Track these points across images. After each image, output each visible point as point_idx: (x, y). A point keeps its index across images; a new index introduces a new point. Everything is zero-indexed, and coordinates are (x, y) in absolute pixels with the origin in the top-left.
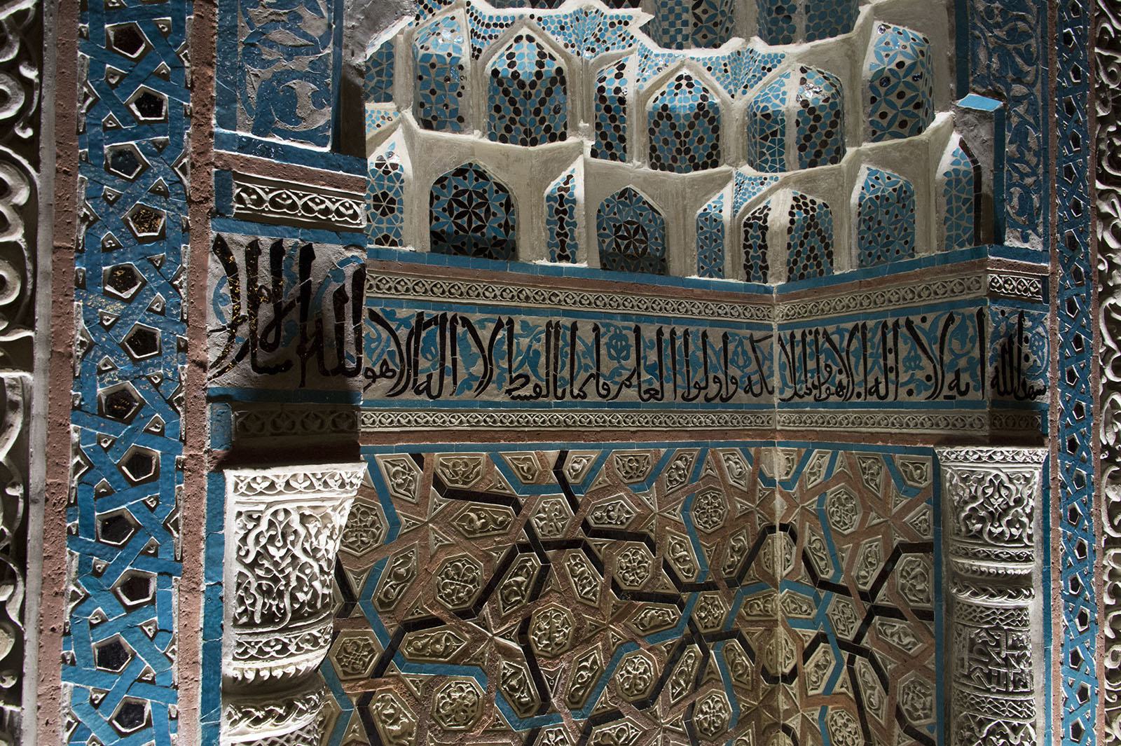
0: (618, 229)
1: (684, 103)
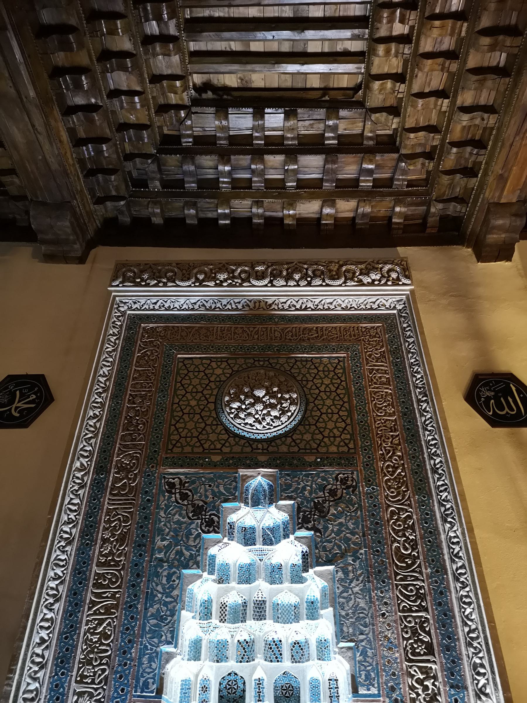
0: (282, 687)
1: (300, 638)
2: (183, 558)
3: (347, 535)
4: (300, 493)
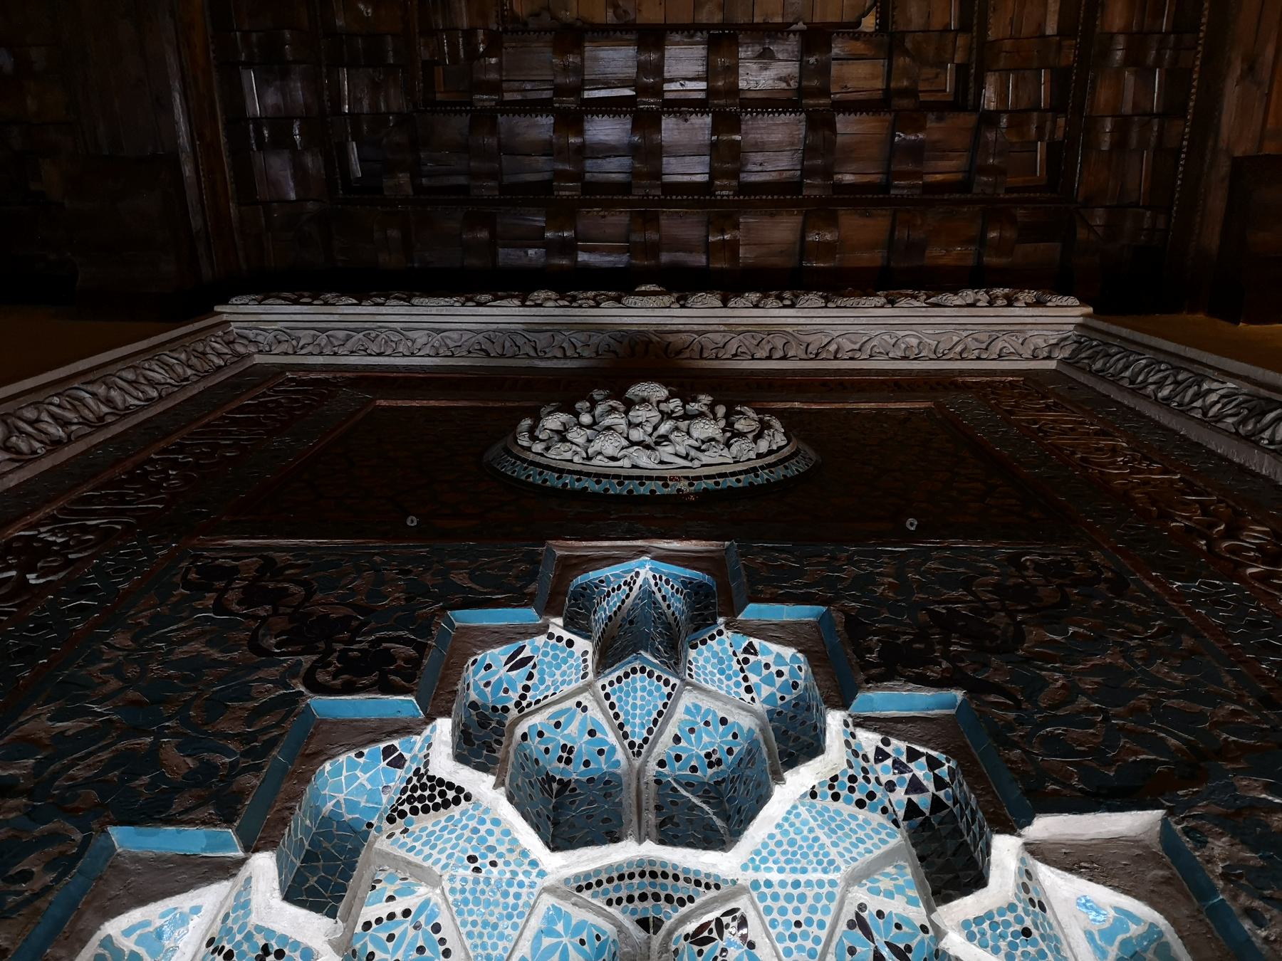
2: (146, 779)
3: (1167, 702)
4: (845, 589)
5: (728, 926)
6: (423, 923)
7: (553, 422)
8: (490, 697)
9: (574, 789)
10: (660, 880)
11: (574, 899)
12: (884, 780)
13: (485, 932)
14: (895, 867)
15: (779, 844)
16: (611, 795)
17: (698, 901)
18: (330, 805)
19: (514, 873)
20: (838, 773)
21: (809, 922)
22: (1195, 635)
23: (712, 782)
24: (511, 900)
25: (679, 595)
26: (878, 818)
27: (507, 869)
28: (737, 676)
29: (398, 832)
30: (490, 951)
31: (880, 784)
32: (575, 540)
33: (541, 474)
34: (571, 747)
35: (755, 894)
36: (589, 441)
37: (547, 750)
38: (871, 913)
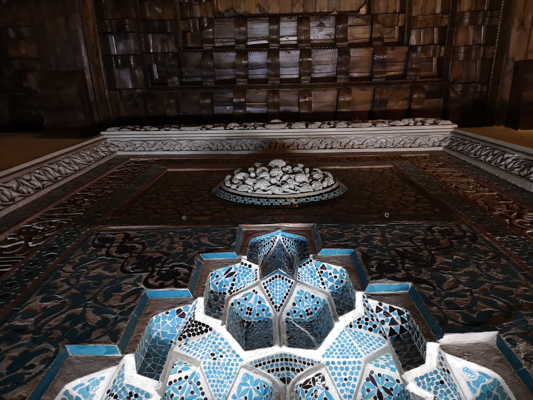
5: (317, 380)
6: (193, 381)
7: (240, 176)
8: (218, 288)
9: (253, 325)
10: (289, 362)
11: (254, 370)
12: (380, 319)
13: (218, 384)
14: (386, 355)
15: (337, 346)
16: (268, 327)
17: (305, 370)
18: (155, 334)
19: (230, 360)
20: (361, 317)
21: (350, 378)
22: (507, 259)
23: (309, 321)
24: (229, 371)
25: (293, 246)
26: (378, 335)
27: (227, 358)
28: (318, 278)
29: (183, 344)
30: (220, 392)
31: (378, 321)
32: (250, 224)
33: (235, 197)
34: (251, 308)
35: (328, 367)
36: (255, 184)
37: (242, 310)
38: (375, 375)
